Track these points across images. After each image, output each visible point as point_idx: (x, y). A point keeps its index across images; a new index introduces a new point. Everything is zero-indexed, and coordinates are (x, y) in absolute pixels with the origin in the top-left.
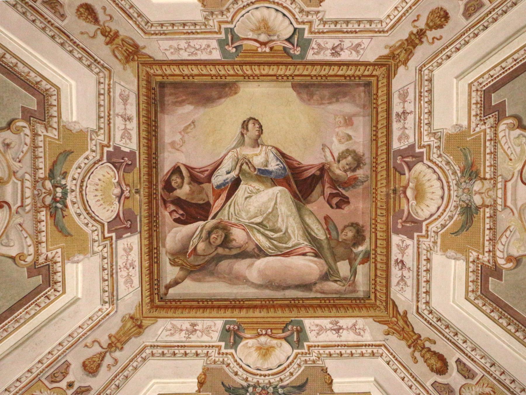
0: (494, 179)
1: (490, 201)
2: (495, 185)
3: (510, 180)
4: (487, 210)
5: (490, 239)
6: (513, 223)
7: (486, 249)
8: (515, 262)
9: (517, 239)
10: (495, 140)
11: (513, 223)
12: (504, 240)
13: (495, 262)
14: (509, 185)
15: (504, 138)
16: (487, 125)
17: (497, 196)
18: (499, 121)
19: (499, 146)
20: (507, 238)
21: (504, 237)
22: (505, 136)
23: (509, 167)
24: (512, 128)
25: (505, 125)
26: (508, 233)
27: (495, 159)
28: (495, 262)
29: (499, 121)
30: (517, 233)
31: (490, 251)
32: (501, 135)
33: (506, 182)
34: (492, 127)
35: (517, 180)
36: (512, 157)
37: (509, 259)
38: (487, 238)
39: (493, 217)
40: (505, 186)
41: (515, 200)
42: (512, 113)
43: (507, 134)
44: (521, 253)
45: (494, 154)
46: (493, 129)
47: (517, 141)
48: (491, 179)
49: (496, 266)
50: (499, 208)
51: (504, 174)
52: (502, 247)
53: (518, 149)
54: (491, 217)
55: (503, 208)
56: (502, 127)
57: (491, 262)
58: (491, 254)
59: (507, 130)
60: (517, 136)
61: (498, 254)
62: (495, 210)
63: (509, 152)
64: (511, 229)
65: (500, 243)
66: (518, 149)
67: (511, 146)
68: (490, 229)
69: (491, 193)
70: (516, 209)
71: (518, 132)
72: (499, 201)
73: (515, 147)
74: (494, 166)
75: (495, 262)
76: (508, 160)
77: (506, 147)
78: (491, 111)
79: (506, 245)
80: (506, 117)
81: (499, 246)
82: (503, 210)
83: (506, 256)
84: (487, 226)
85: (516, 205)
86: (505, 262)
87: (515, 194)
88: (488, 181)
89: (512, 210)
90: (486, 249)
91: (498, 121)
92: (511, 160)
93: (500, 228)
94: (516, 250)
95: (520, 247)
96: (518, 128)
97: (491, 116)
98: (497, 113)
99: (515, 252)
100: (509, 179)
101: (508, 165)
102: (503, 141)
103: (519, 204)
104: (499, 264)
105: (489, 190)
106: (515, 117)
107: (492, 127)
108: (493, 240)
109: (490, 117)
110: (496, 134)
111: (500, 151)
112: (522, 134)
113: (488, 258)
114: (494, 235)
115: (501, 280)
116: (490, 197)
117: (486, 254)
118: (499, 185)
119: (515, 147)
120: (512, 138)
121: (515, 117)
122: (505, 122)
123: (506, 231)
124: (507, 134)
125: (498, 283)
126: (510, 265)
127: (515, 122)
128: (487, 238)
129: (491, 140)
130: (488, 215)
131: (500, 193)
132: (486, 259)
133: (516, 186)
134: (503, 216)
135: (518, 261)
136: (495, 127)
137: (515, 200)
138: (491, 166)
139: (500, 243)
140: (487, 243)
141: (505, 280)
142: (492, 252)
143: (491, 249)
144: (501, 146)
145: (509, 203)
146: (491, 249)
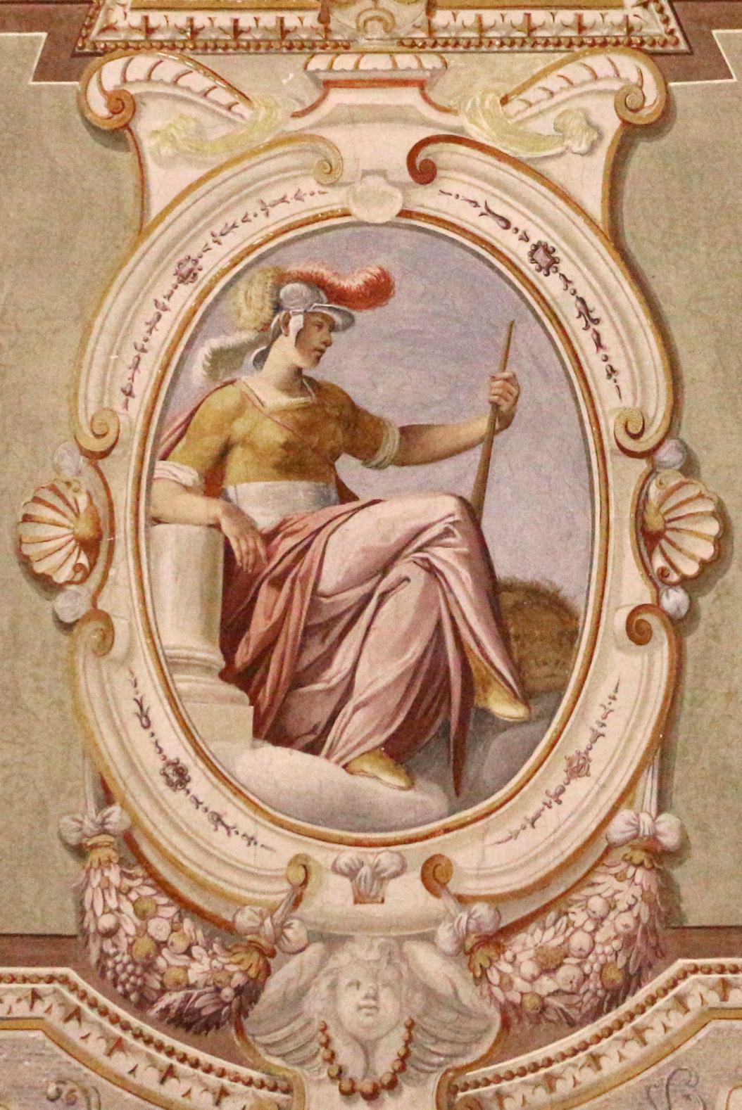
0: (434, 42)
1: (344, 27)
2: (411, 46)
3: (426, 98)
4: (311, 19)
5: (195, 32)
6: (263, 112)
7: (156, 19)
8: (115, 122)
9: (200, 131)
10: (581, 42)
11: (263, 112)
12: (198, 81)
13: (106, 51)
14: (410, 97)
15: (586, 75)
16: (639, 10)
17: (363, 53)
18: (653, 55)
19: (559, 57)
20: (205, 94)
21: (208, 83)
22: (596, 78)
23: (475, 93)
24: (625, 102)
25: (634, 78)
26: (224, 97)
27: (509, 43)
28: (106, 51)
29: (653, 55)
30: (223, 130)
31: (149, 31)
32: (599, 62)
33: (421, 85)
34: (630, 30)
35: (427, 123)
36: (515, 105)
37: (124, 103)
38: (201, 19)
39: (285, 42)
40: (405, 83)
41: (353, 121)
42: (680, 101)
43: (600, 85)
44: (148, 145)
45: (529, 39)
46: (621, 33)
47: (575, 124)
48: (431, 30)
49: (95, 54)
50: (319, 63)
51: (449, 76)
52: (169, 78)
53: (544, 126)
54: (284, 32)
55: (322, 76)
56: (630, 66)
57: (109, 37)
58: (139, 37)
59: (617, 86)
60: (595, 119)
61: (141, 64)
62: (309, 47)
63: (532, 94)
64: (240, 108)
65: (180, 68)
66: (544, 126)
67: (558, 98)
68: (237, 31)
69: (377, 31)
70: (319, 124)
71: (611, 125)
72: (345, 62)
73: (553, 115)
74: (480, 42)
75: (105, 53)
76: (509, 88)
77: (552, 82)
78: (691, 28)
79: (178, 92)
80: (664, 78)
81: (170, 67)
82: (313, 75)
83: (133, 90)
84: (246, 20)
85: (331, 122)
86: (109, 87)
87: (372, 121)
88: (422, 18)
89: (313, 107)
90: (156, 19)
91: (654, 53)
92: (505, 101)
93: (242, 69)
94: (158, 124)
95: (173, 140)
96: (625, 123)
97: (673, 24)
98: (683, 46)
99: (148, 124)
100: (431, 95)
101: (486, 91)
102: (575, 71)
103: (334, 135)
104: (99, 68)
105: (389, 25)
106: (667, 112)
107: (630, 30)
108: (191, 43)
109: (666, 21)
110: (604, 44)
111: (540, 61)
112: (601, 136)
113: (122, 24)
114: (214, 47)
115: (41, 74)
116: (362, 28)
117: (136, 19)
118: (406, 60)
119: (553, 115)
120: (588, 103)
121: (667, 112)
122: (649, 77)
123: (231, 88)
124: (600, 85)
125: (25, 66)
126: (99, 107)
127: (644, 112)
128: (201, 19)
129: (581, 28)
130: (291, 20)
131: (377, 64)
132: (117, 16)
133: (406, 121)
134: (288, 77)
135: (118, 132)
136: (631, 42)
137: (352, 118)
138: (481, 29)
139: (180, 68)
140: (180, 19)
141: (38, 91)
142: (147, 40)
143: (158, 36)
144: (561, 64)
145: (338, 97)
146: (158, 36)
